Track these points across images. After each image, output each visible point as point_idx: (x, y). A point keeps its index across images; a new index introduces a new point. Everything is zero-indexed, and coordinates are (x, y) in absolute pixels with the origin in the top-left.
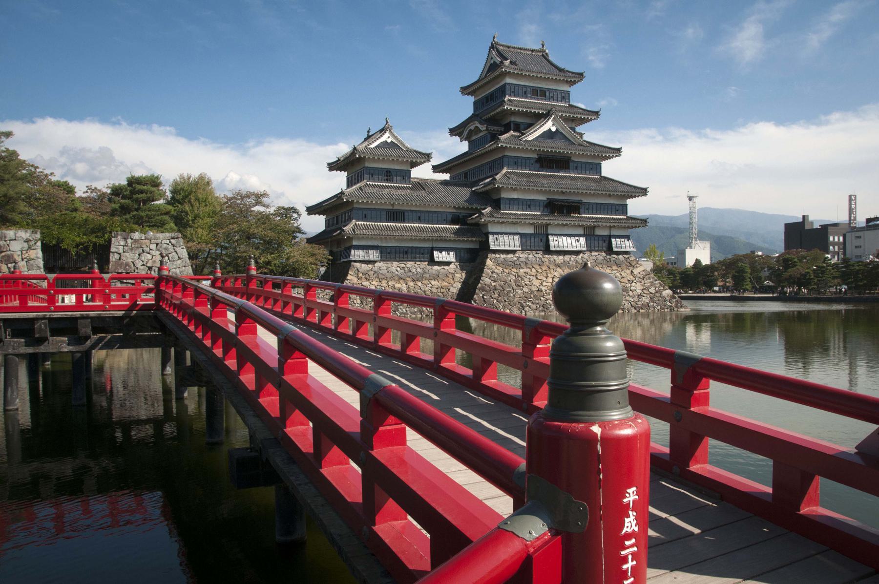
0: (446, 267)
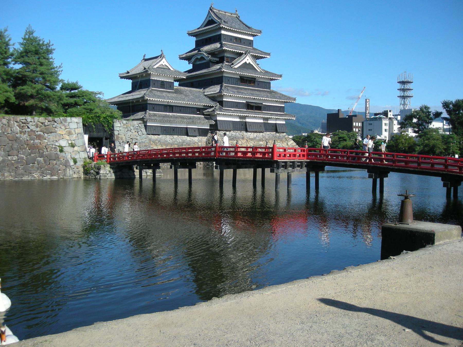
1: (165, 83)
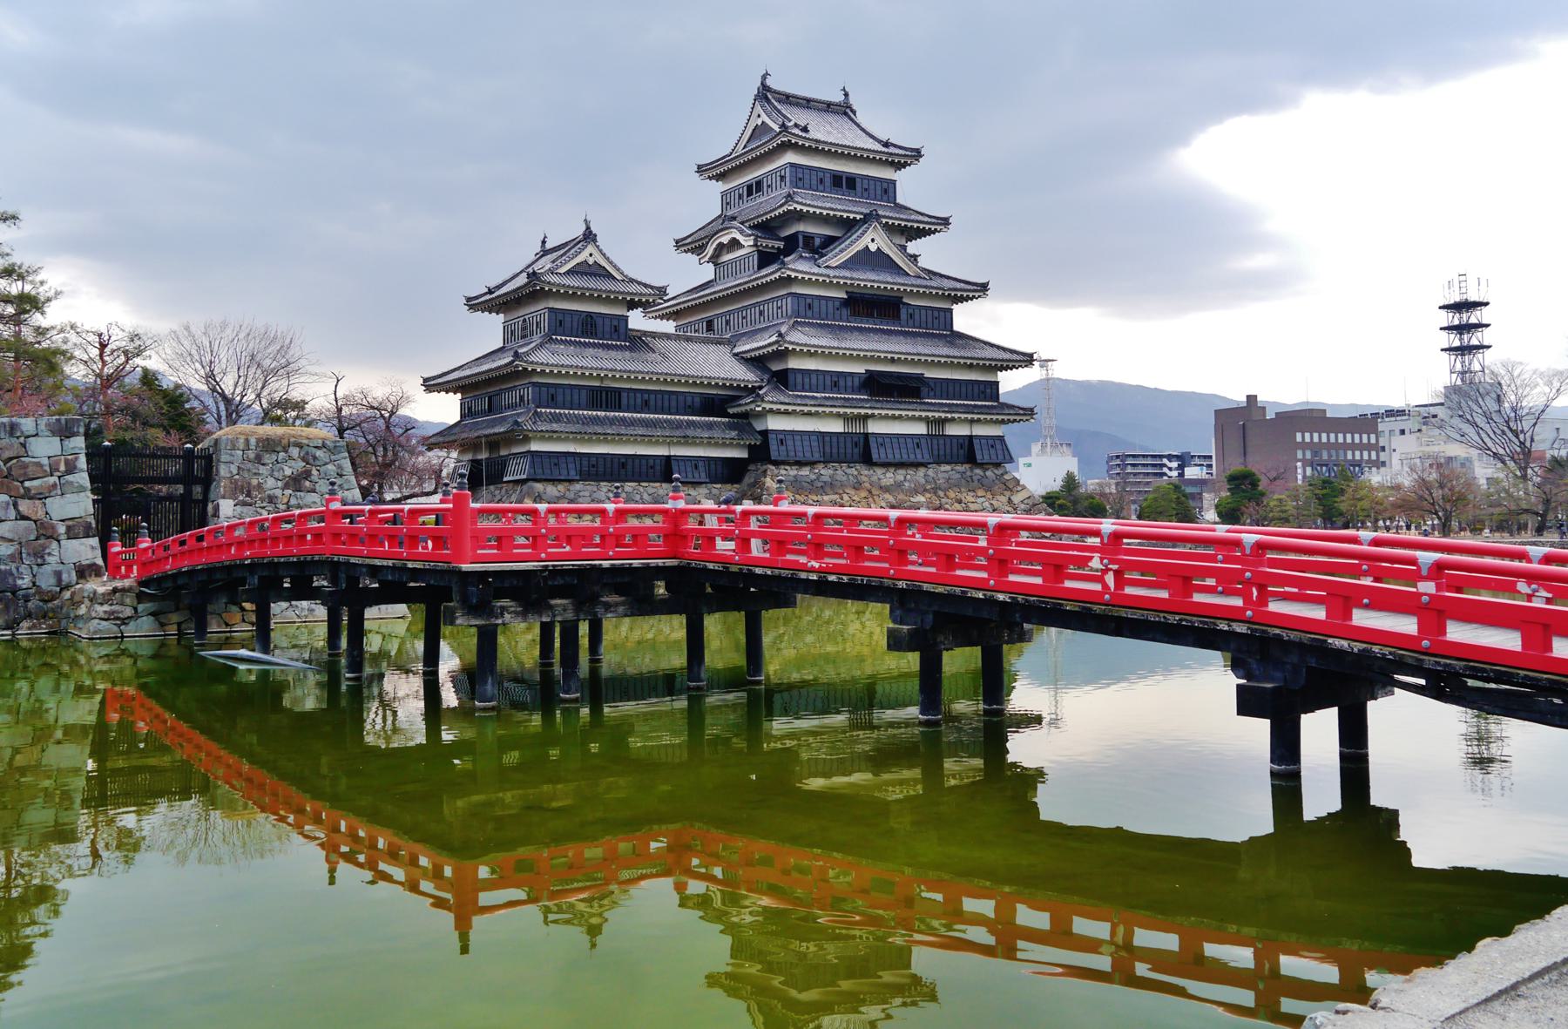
1: (599, 322)
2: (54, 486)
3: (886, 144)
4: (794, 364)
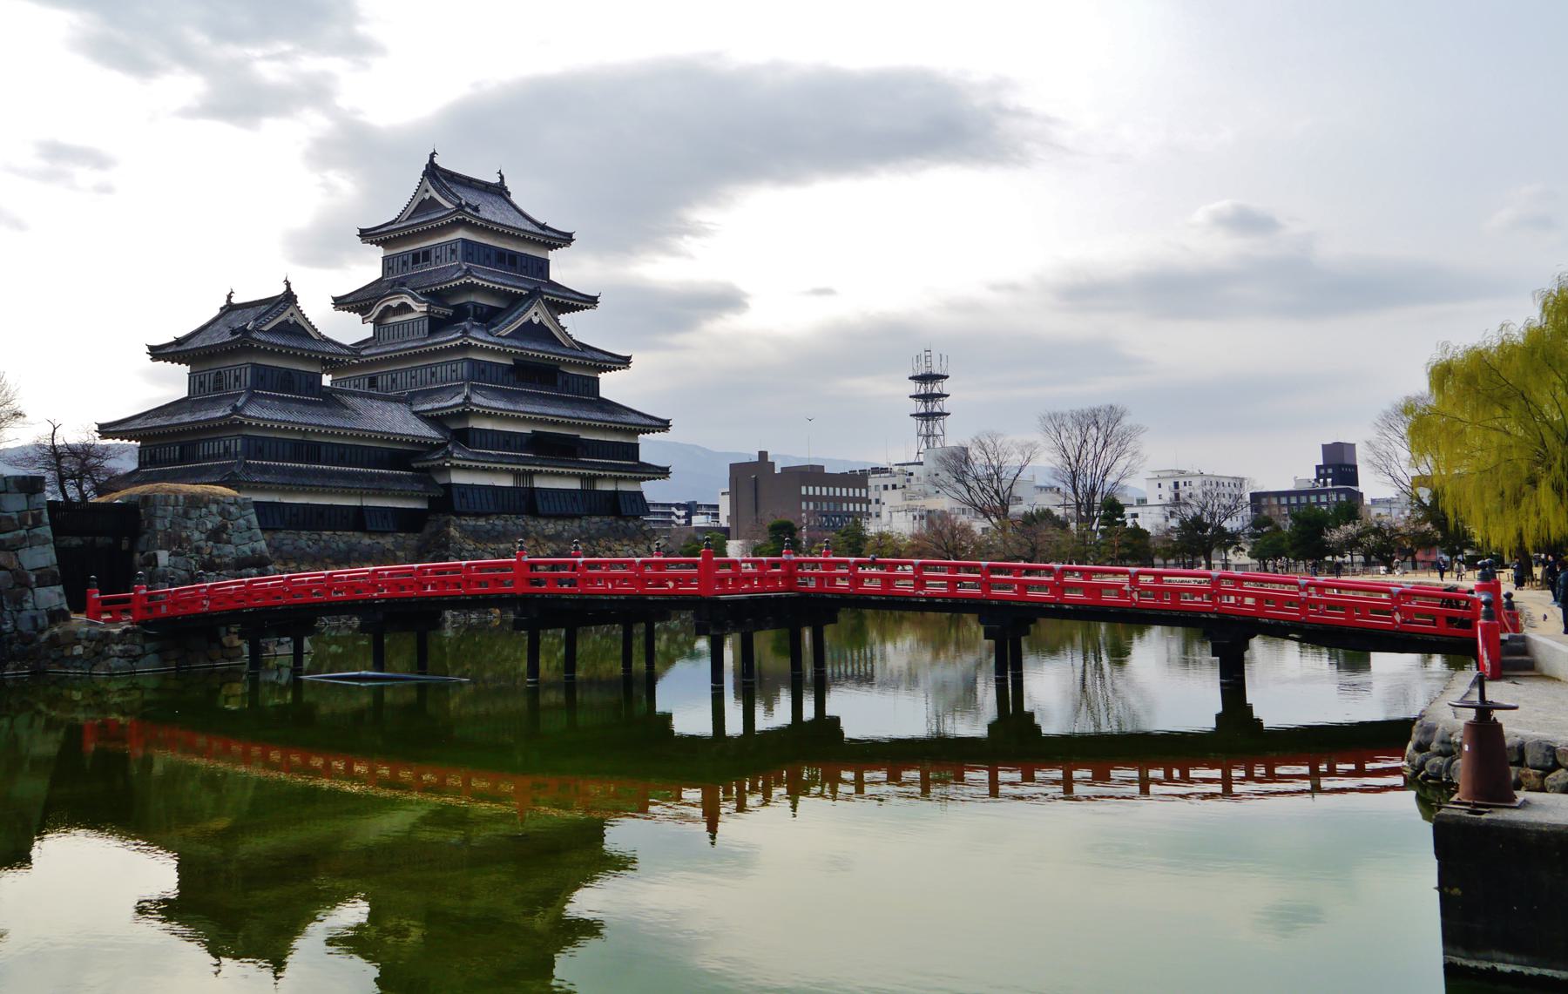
0: (382, 541)
2: (24, 539)
3: (543, 227)
4: (475, 424)
